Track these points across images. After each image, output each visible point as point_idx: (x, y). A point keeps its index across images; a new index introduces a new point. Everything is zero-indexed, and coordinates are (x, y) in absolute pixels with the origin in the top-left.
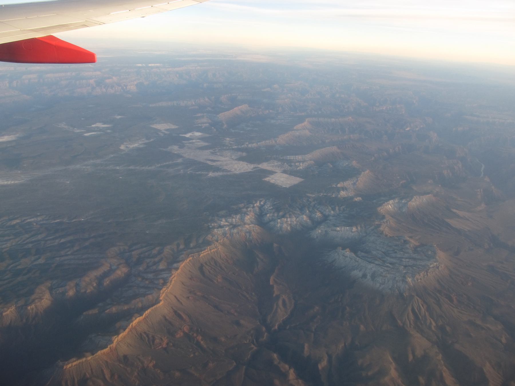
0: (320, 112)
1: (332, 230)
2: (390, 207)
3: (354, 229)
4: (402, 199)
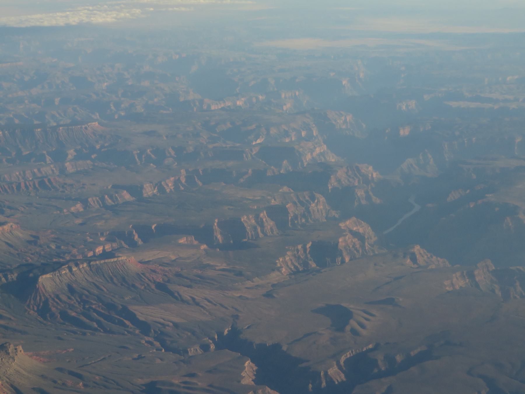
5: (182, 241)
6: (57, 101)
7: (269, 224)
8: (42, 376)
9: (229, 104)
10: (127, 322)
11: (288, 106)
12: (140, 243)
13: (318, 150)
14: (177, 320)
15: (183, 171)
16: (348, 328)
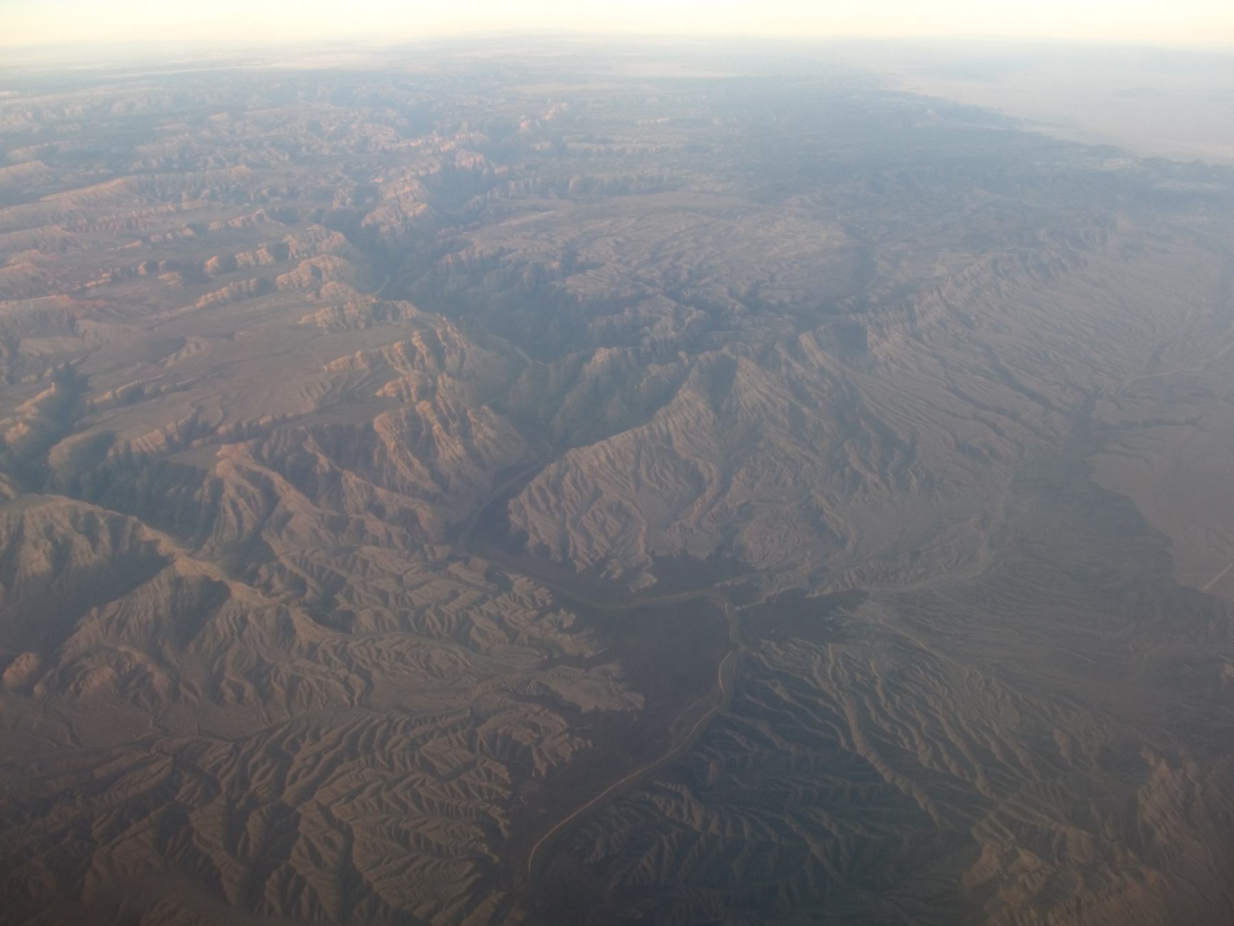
13: (407, 189)
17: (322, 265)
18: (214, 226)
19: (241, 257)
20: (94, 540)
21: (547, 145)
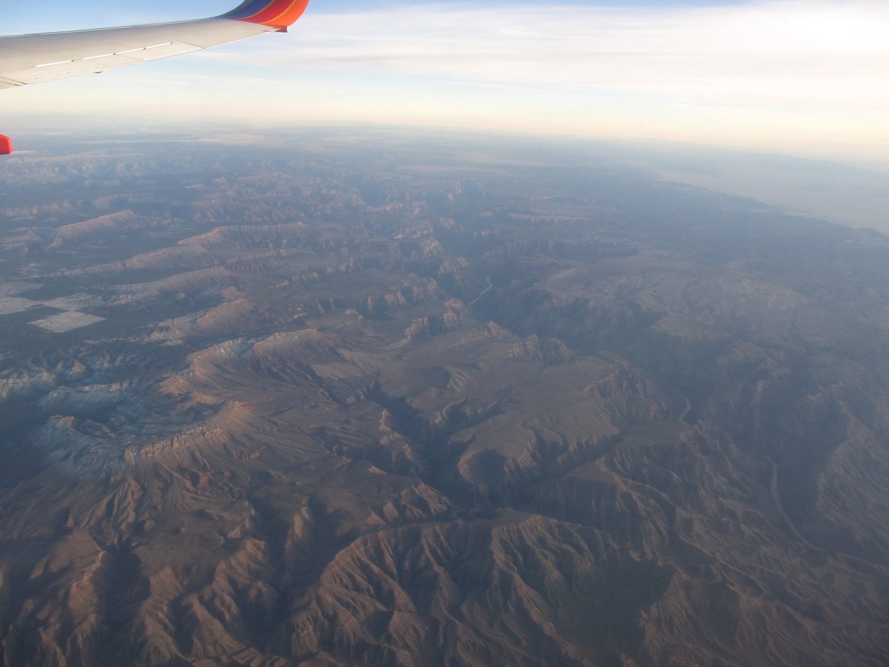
0: (266, 218)
1: (76, 392)
2: (223, 351)
3: (115, 387)
4: (248, 339)
5: (348, 312)
6: (279, 203)
7: (402, 300)
8: (250, 424)
9: (382, 209)
10: (309, 377)
11: (416, 212)
12: (322, 311)
14: (341, 376)
15: (351, 259)
16: (448, 386)
17: (454, 306)
18: (329, 270)
19: (389, 298)
20: (580, 550)
21: (489, 214)
